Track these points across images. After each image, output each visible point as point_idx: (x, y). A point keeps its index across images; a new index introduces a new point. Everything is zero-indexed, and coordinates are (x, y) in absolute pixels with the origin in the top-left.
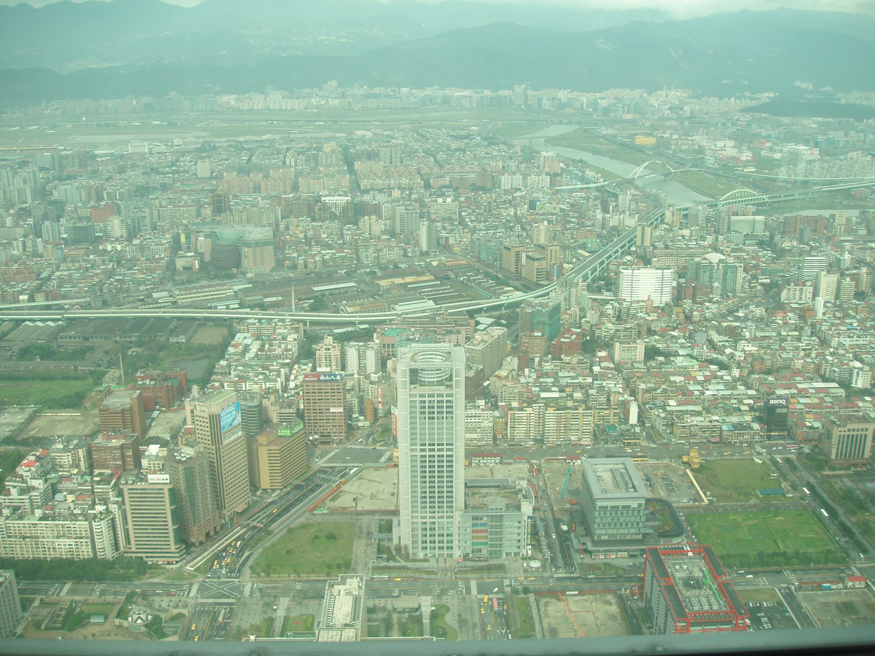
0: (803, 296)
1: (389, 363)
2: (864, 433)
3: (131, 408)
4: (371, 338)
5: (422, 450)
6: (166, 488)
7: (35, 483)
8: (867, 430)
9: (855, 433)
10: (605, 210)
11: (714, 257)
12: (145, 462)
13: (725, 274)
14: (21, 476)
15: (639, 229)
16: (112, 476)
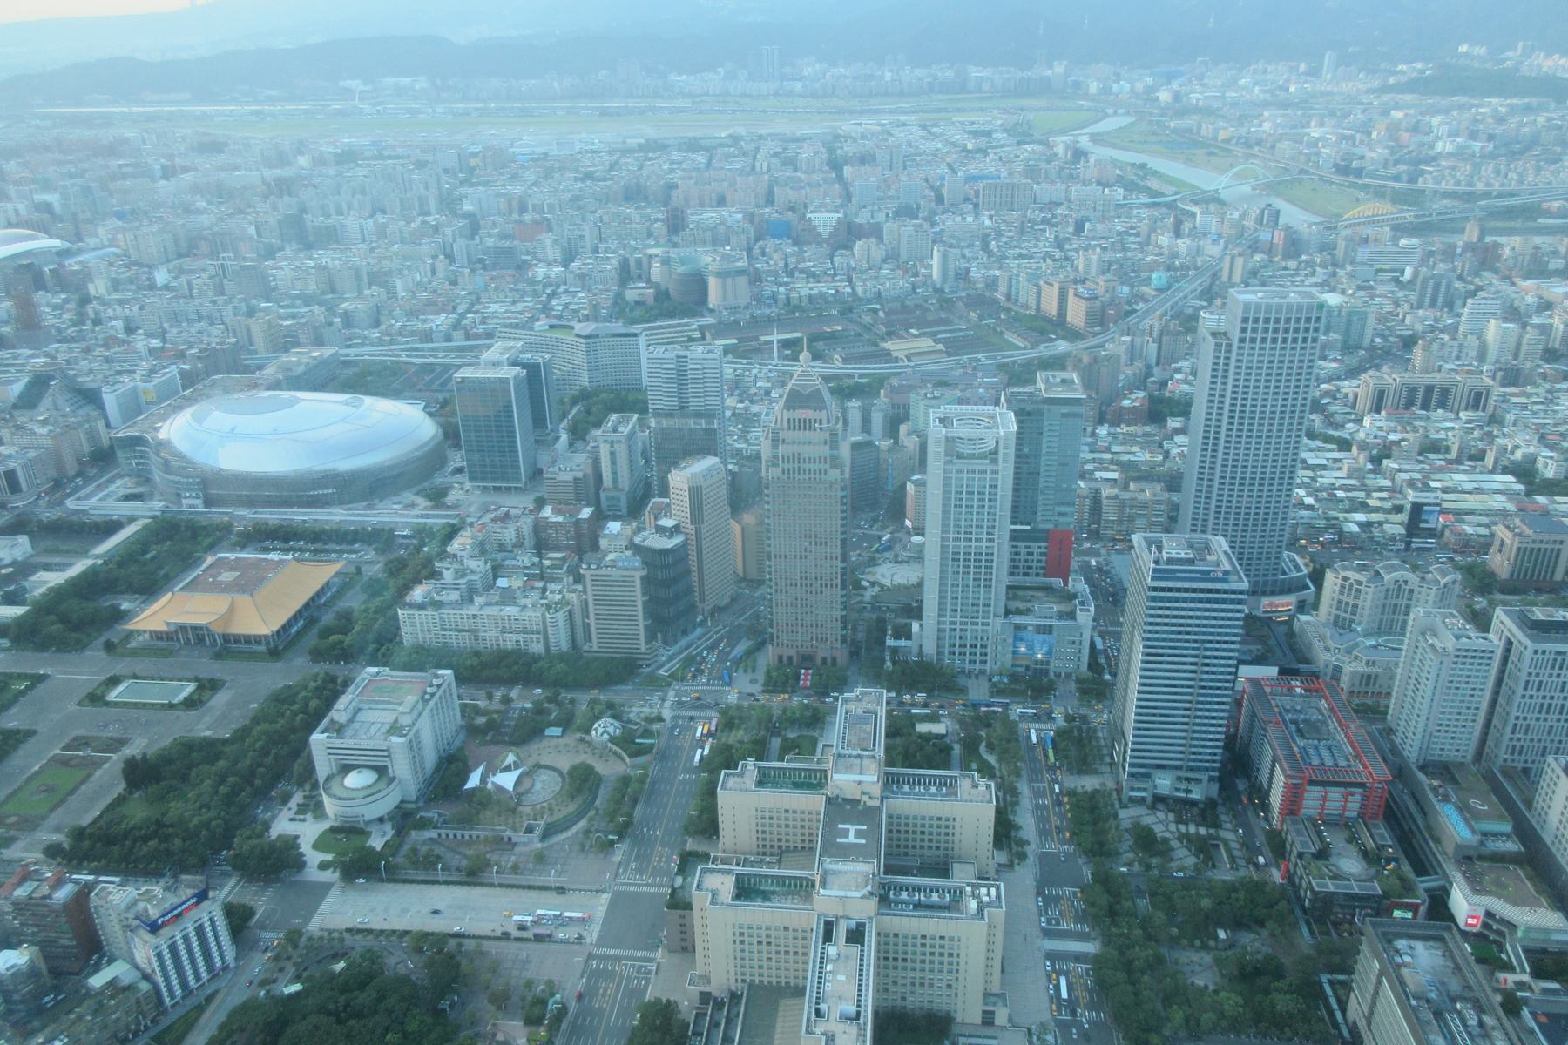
0: (1463, 355)
1: (903, 428)
2: (1557, 546)
3: (585, 476)
4: (877, 395)
5: (956, 539)
6: (638, 575)
7: (473, 564)
8: (1561, 542)
9: (1543, 546)
10: (1178, 233)
11: (1333, 299)
12: (603, 543)
13: (1349, 322)
14: (455, 556)
15: (1228, 259)
16: (564, 559)
